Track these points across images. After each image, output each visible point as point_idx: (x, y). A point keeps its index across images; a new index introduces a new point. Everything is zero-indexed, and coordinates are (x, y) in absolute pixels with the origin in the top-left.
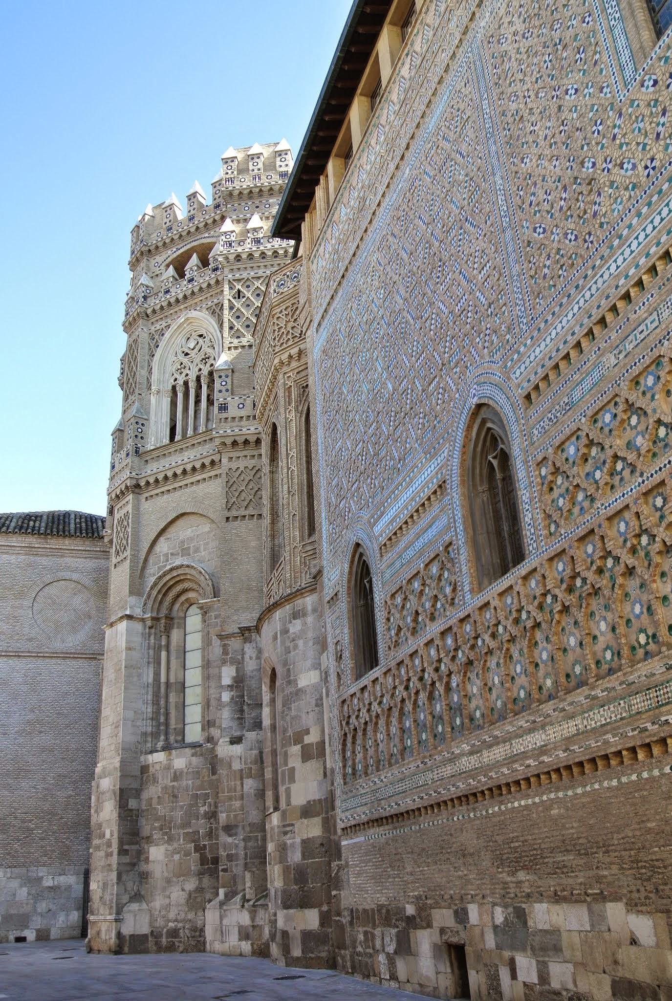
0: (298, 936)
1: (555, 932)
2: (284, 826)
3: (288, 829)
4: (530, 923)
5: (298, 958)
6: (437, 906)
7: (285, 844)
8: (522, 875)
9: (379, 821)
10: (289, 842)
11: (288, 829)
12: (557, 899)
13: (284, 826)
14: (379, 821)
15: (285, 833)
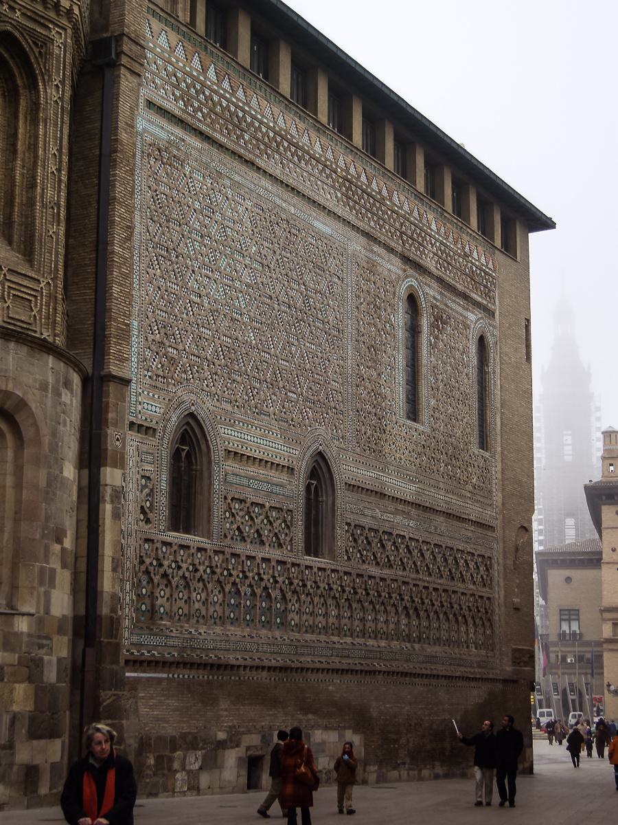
0: (48, 766)
1: (323, 743)
2: (39, 637)
3: (45, 642)
4: (312, 740)
5: (46, 795)
6: (249, 732)
7: (41, 660)
8: (310, 716)
9: (191, 665)
10: (46, 658)
11: (45, 642)
12: (326, 728)
13: (39, 637)
14: (191, 665)
15: (41, 646)
